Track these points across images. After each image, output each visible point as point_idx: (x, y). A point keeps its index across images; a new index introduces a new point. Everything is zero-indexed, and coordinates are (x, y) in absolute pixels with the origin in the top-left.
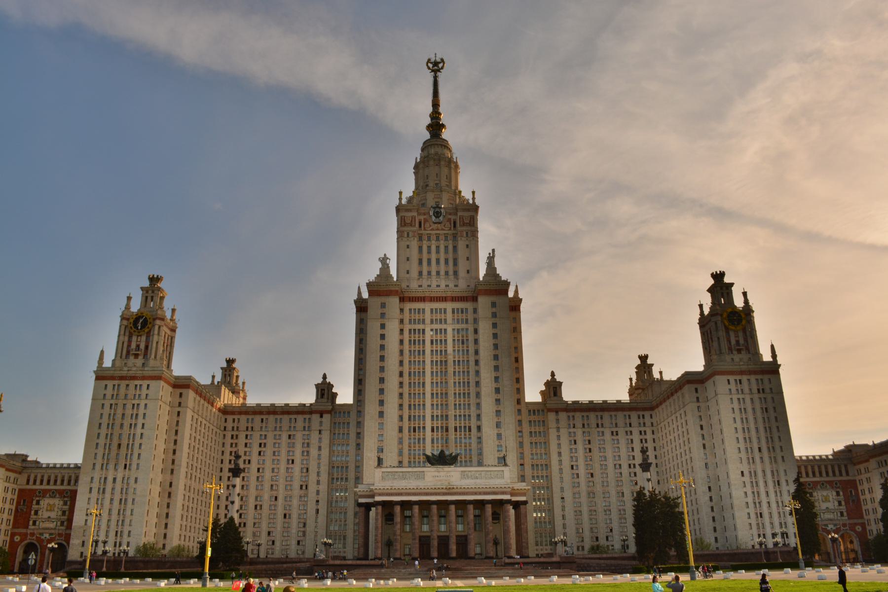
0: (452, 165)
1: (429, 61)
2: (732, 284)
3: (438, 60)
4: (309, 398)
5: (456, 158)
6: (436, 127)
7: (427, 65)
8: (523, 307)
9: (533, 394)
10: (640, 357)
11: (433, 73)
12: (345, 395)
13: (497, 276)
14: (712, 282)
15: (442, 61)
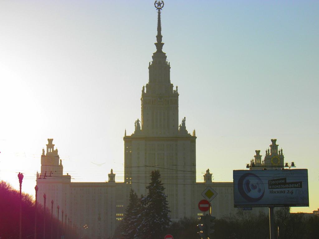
0: (168, 67)
1: (156, 2)
2: (278, 145)
3: (161, 2)
4: (106, 179)
5: (169, 62)
6: (159, 45)
7: (155, 5)
8: (197, 140)
9: (200, 179)
10: (256, 151)
11: (157, 11)
12: (120, 178)
13: (186, 132)
14: (271, 143)
15: (163, 2)
